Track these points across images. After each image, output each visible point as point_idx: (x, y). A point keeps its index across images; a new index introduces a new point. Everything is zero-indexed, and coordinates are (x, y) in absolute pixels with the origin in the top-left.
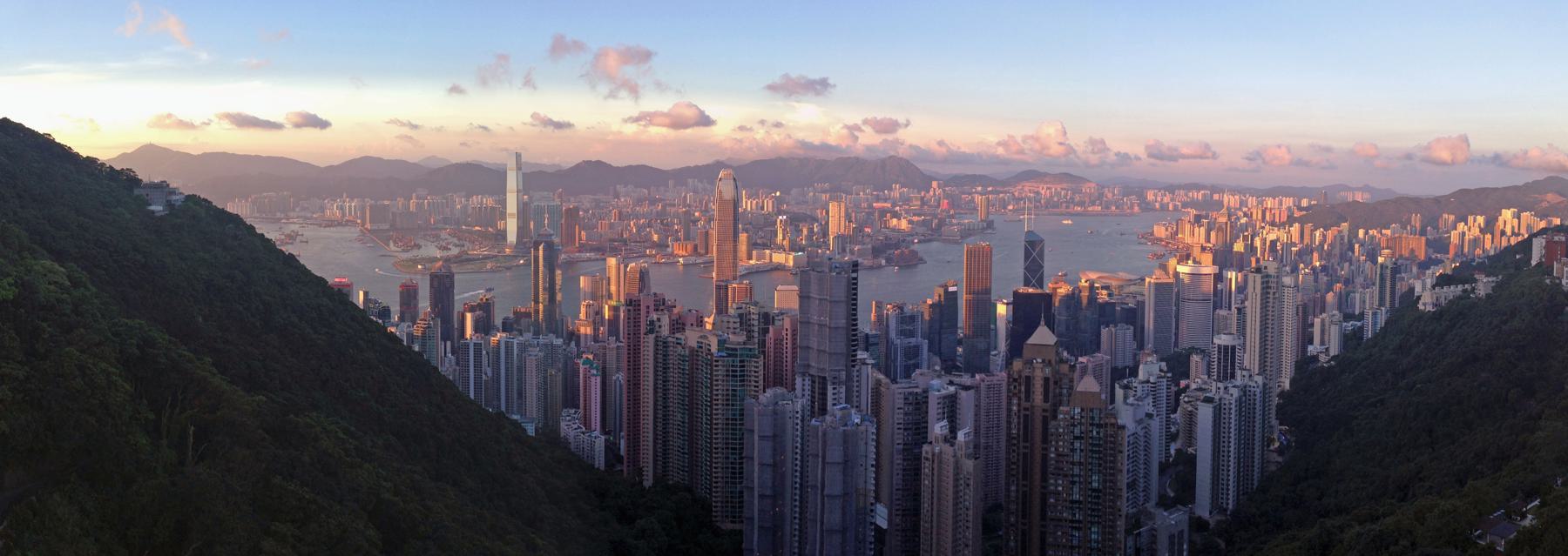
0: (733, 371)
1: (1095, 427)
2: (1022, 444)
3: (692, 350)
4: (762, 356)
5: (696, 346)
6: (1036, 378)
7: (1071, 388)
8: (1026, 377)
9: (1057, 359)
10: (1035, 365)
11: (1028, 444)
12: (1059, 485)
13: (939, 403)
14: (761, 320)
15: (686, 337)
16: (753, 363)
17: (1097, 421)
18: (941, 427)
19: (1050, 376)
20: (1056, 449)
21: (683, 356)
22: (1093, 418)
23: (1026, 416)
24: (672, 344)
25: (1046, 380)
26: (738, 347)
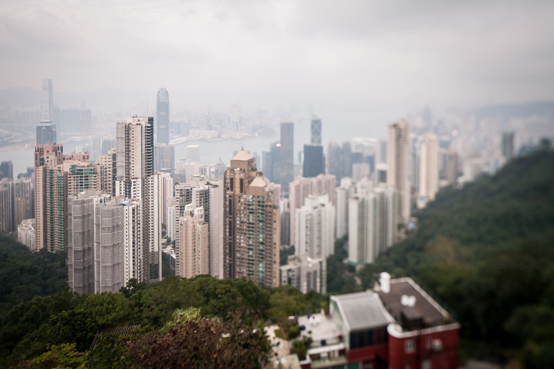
0: (81, 182)
3: (66, 174)
5: (69, 172)
6: (237, 179)
9: (250, 168)
11: (232, 216)
12: (242, 239)
13: (196, 195)
15: (63, 166)
16: (93, 178)
17: (261, 204)
18: (188, 207)
19: (243, 178)
20: (240, 219)
21: (60, 177)
22: (259, 202)
23: (230, 200)
24: (55, 171)
25: (241, 180)
26: (84, 168)
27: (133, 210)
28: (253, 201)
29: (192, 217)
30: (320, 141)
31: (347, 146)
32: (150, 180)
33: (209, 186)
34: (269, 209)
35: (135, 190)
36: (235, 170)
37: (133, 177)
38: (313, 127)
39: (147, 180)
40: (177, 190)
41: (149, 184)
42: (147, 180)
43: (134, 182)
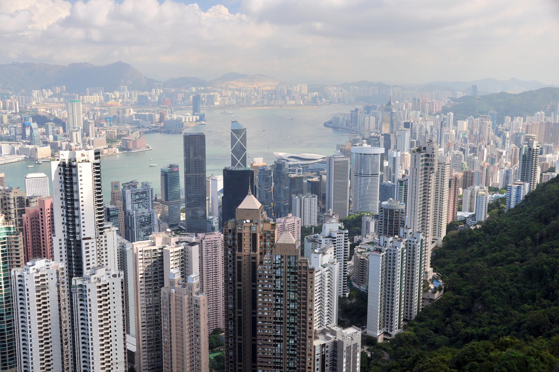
1: (291, 269)
2: (237, 283)
4: (21, 233)
7: (273, 241)
8: (238, 233)
9: (262, 219)
10: (244, 225)
14: (16, 204)
20: (263, 286)
22: (290, 263)
25: (254, 236)
27: (122, 283)
28: (283, 262)
29: (184, 287)
30: (244, 162)
31: (279, 166)
32: (103, 239)
33: (184, 243)
34: (303, 272)
35: (87, 254)
36: (244, 222)
37: (83, 237)
38: (233, 140)
39: (99, 240)
40: (140, 251)
41: (102, 245)
42: (99, 240)
43: (87, 244)
